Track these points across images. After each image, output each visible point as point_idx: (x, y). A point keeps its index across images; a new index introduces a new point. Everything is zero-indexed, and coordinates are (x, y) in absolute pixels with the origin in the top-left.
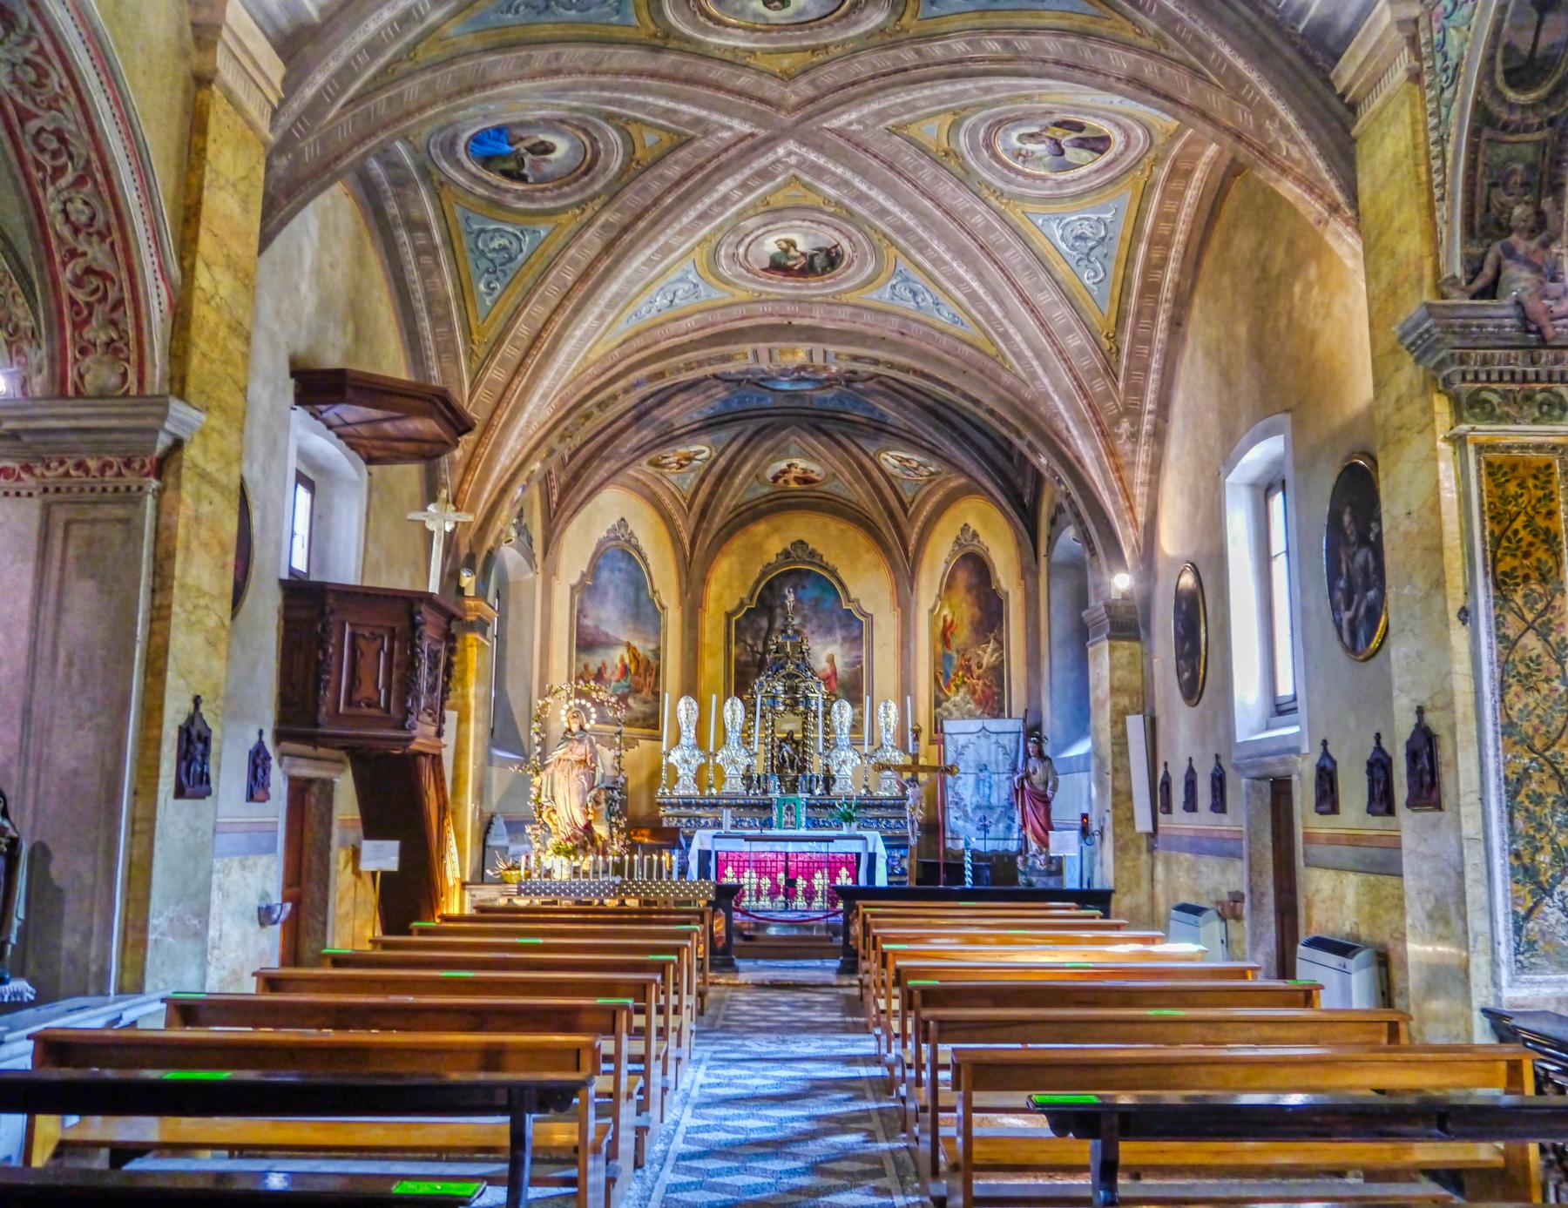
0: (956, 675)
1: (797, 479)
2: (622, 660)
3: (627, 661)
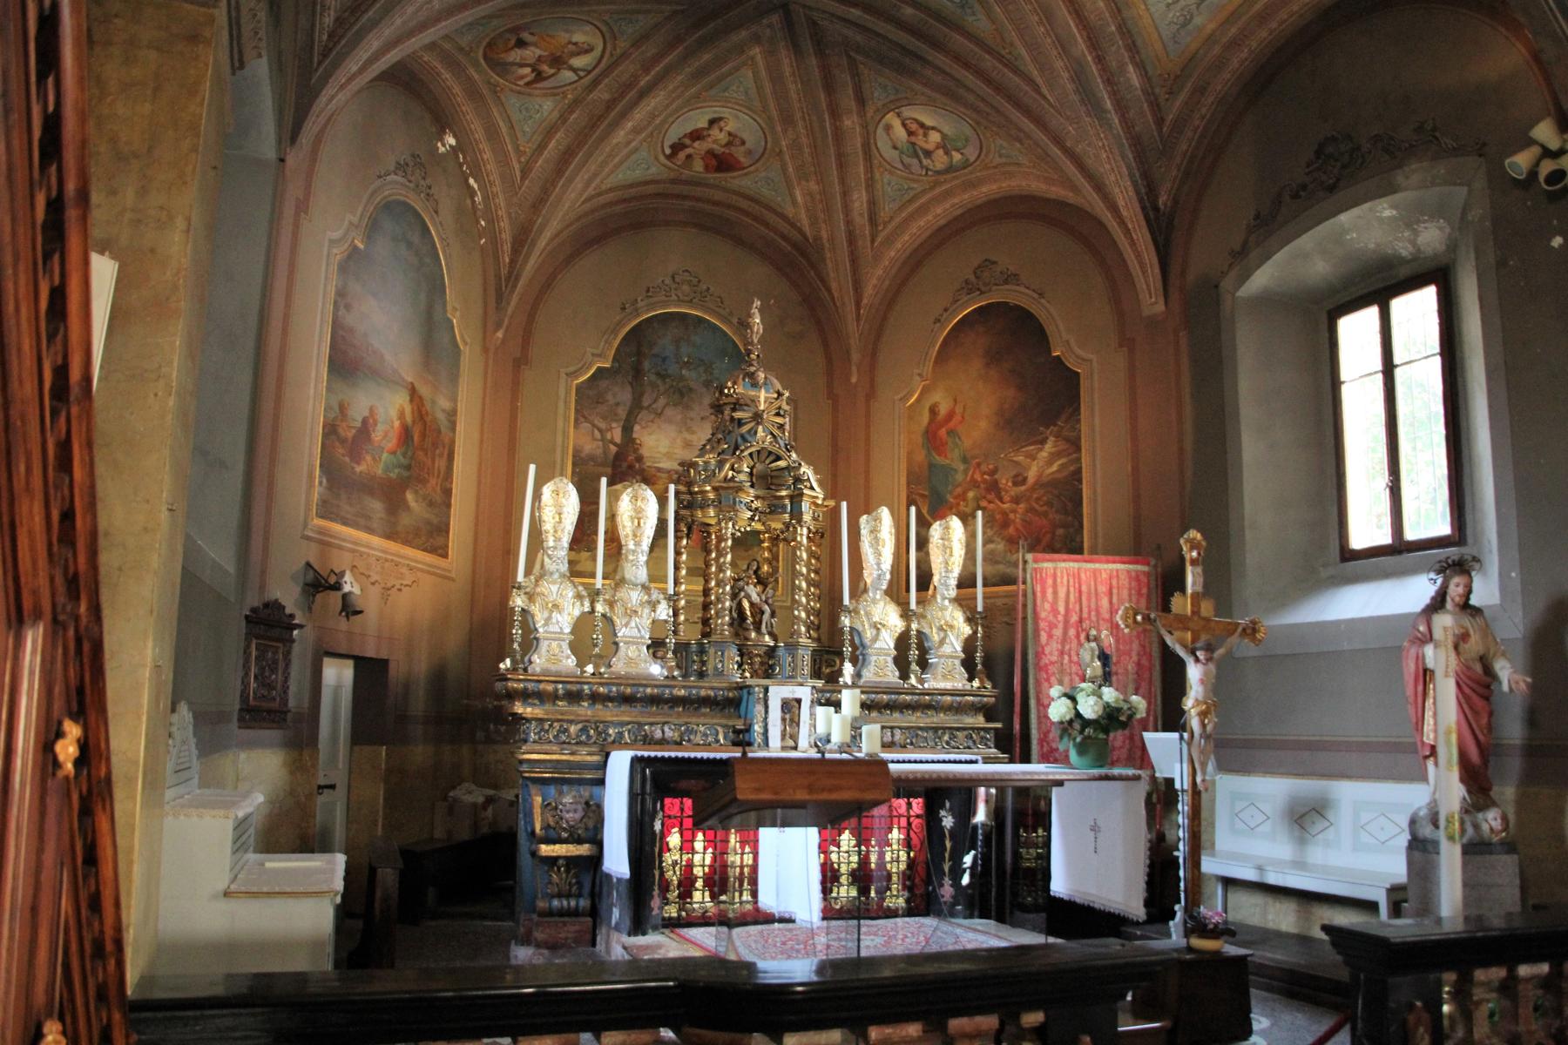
0: (963, 497)
1: (711, 153)
2: (402, 415)
3: (409, 419)
